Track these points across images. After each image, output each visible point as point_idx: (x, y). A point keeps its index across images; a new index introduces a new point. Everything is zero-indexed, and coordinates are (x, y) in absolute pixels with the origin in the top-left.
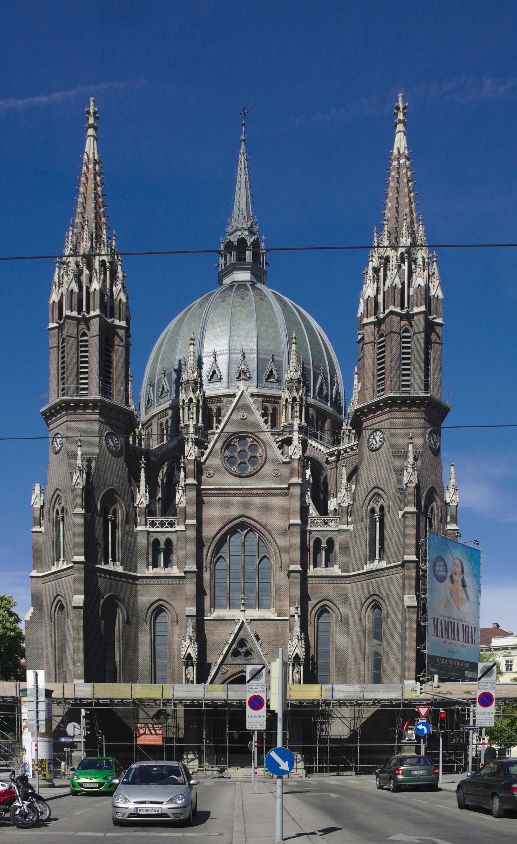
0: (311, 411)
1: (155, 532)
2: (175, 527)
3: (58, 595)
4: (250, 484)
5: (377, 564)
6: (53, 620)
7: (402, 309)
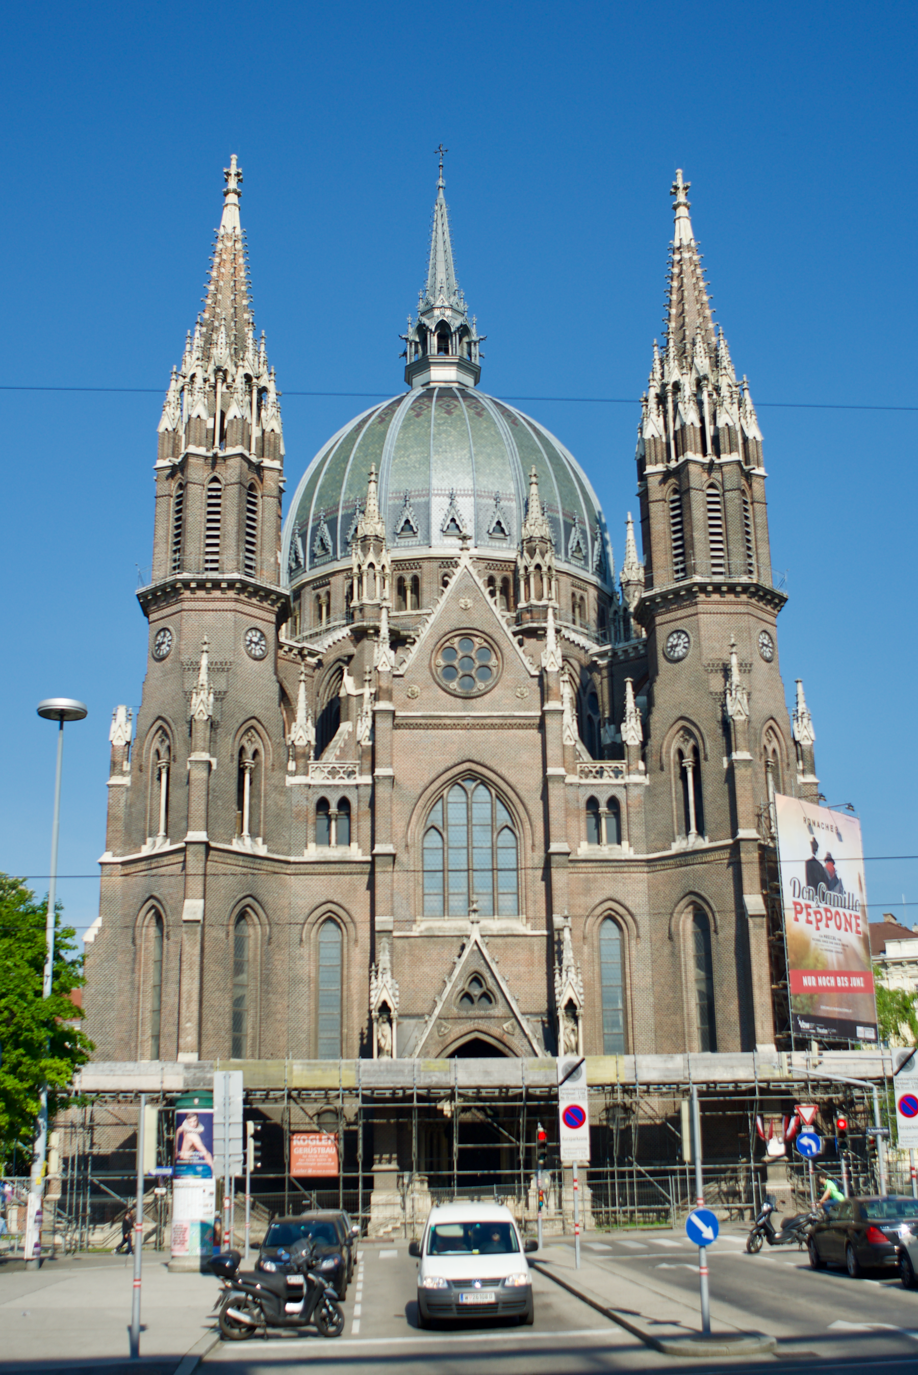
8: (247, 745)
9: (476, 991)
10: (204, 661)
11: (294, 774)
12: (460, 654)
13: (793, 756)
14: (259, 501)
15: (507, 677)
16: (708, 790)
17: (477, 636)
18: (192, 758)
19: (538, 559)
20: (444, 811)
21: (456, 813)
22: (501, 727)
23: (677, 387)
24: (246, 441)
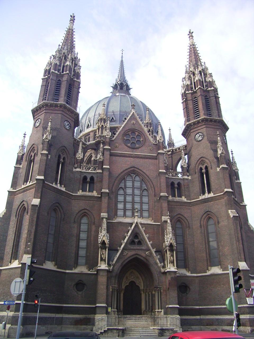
3: (23, 201)
5: (207, 196)
6: (17, 217)
7: (204, 88)
8: (61, 155)
9: (136, 240)
11: (76, 168)
12: (131, 137)
15: (147, 144)
16: (212, 178)
17: (137, 132)
19: (149, 128)
21: (129, 184)
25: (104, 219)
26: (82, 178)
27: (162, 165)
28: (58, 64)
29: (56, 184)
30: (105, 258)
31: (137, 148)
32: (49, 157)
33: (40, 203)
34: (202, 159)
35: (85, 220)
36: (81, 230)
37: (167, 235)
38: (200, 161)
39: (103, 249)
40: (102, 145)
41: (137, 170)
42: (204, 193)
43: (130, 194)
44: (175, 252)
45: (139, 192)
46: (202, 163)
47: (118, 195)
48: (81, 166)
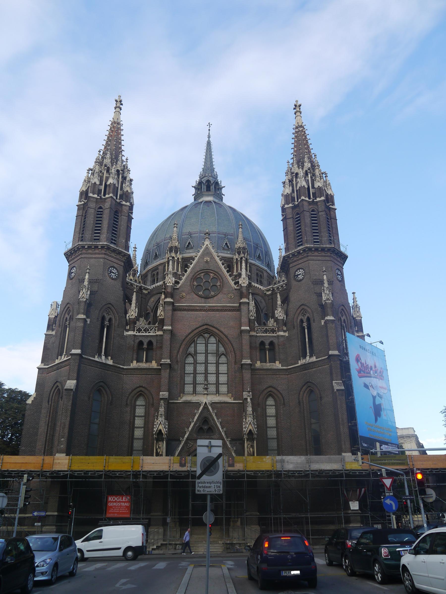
0: (253, 267)
1: (140, 336)
2: (156, 333)
3: (57, 382)
4: (211, 304)
6: (50, 403)
7: (310, 198)
9: (206, 427)
10: (87, 277)
11: (127, 331)
13: (353, 324)
14: (120, 218)
15: (225, 290)
16: (315, 335)
18: (78, 317)
20: (195, 347)
21: (201, 348)
22: (221, 310)
23: (297, 174)
24: (115, 193)
25: (162, 401)
26: (136, 344)
27: (244, 320)
28: (98, 183)
29: (100, 356)
30: (162, 452)
31: (211, 298)
32: (88, 322)
33: (77, 385)
34: (303, 307)
35: (140, 402)
36: (137, 414)
37: (246, 420)
38: (300, 310)
39: (160, 441)
40: (163, 296)
41: (211, 328)
42: (305, 357)
43: (202, 362)
44: (255, 442)
45: (215, 359)
46: (303, 313)
47: (186, 365)
48: (134, 327)
